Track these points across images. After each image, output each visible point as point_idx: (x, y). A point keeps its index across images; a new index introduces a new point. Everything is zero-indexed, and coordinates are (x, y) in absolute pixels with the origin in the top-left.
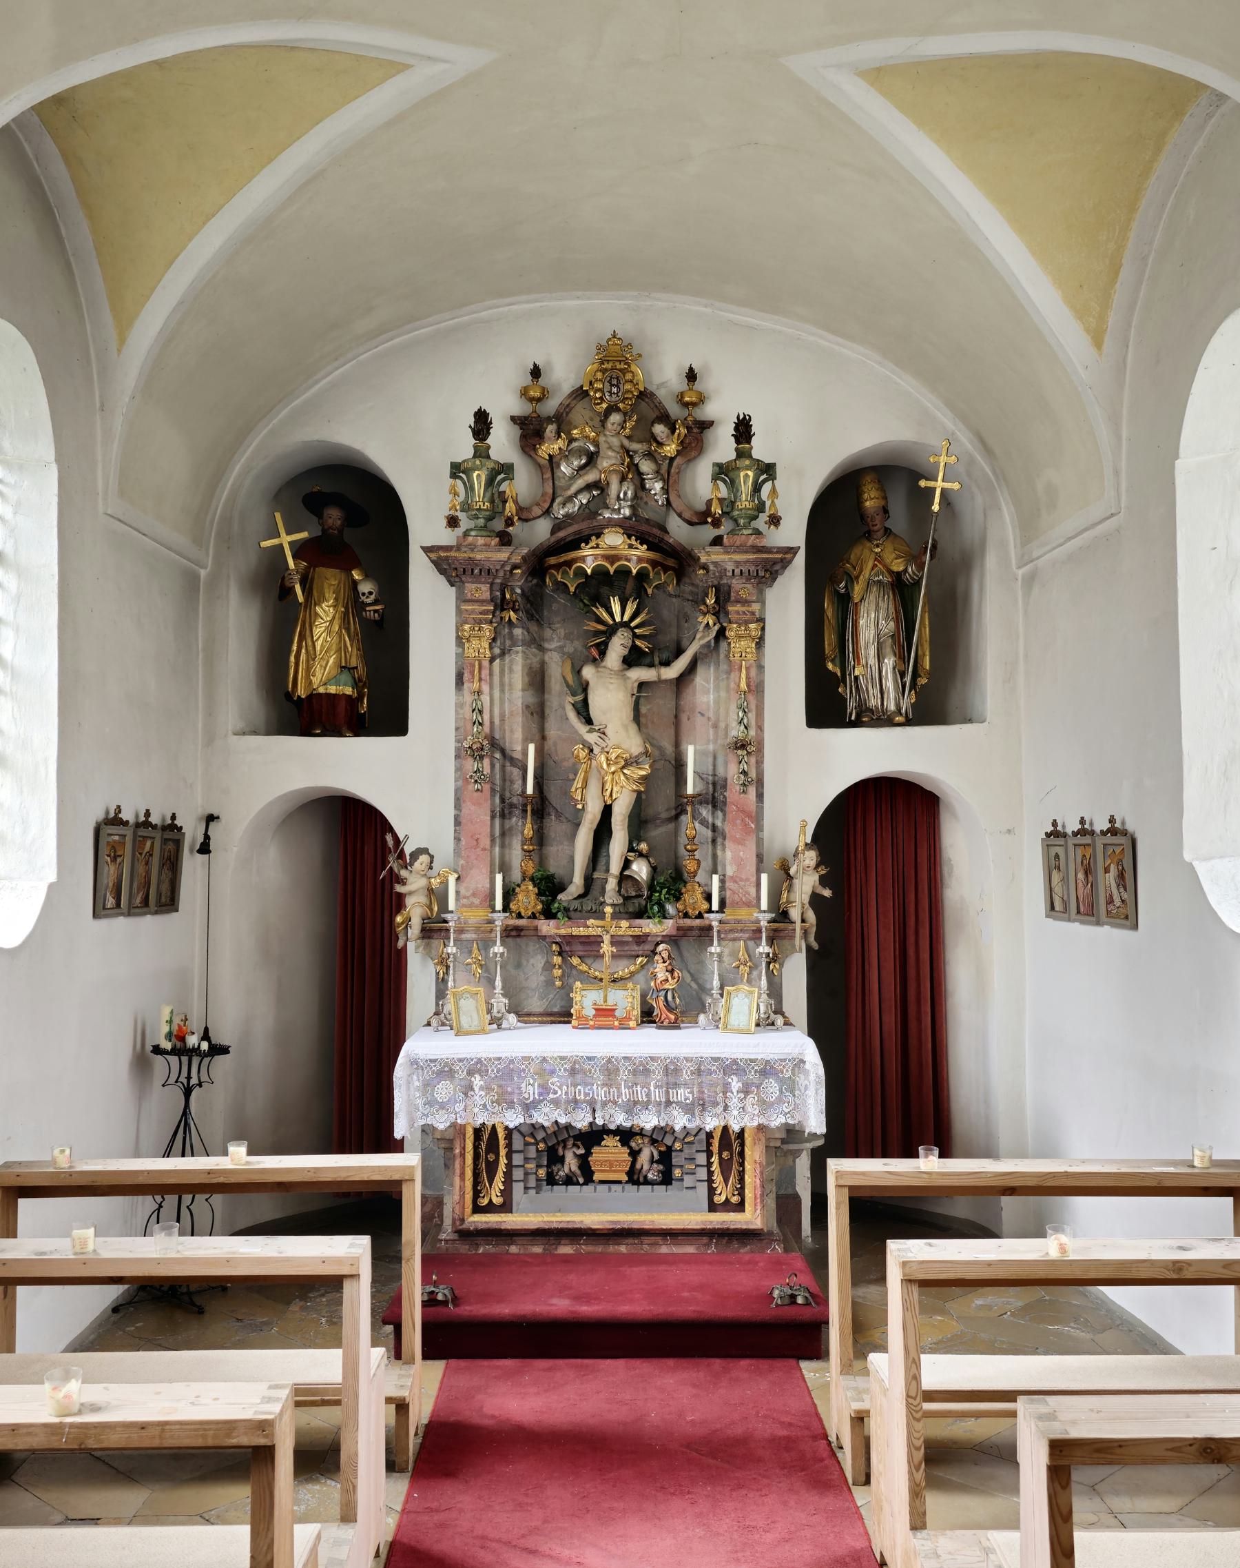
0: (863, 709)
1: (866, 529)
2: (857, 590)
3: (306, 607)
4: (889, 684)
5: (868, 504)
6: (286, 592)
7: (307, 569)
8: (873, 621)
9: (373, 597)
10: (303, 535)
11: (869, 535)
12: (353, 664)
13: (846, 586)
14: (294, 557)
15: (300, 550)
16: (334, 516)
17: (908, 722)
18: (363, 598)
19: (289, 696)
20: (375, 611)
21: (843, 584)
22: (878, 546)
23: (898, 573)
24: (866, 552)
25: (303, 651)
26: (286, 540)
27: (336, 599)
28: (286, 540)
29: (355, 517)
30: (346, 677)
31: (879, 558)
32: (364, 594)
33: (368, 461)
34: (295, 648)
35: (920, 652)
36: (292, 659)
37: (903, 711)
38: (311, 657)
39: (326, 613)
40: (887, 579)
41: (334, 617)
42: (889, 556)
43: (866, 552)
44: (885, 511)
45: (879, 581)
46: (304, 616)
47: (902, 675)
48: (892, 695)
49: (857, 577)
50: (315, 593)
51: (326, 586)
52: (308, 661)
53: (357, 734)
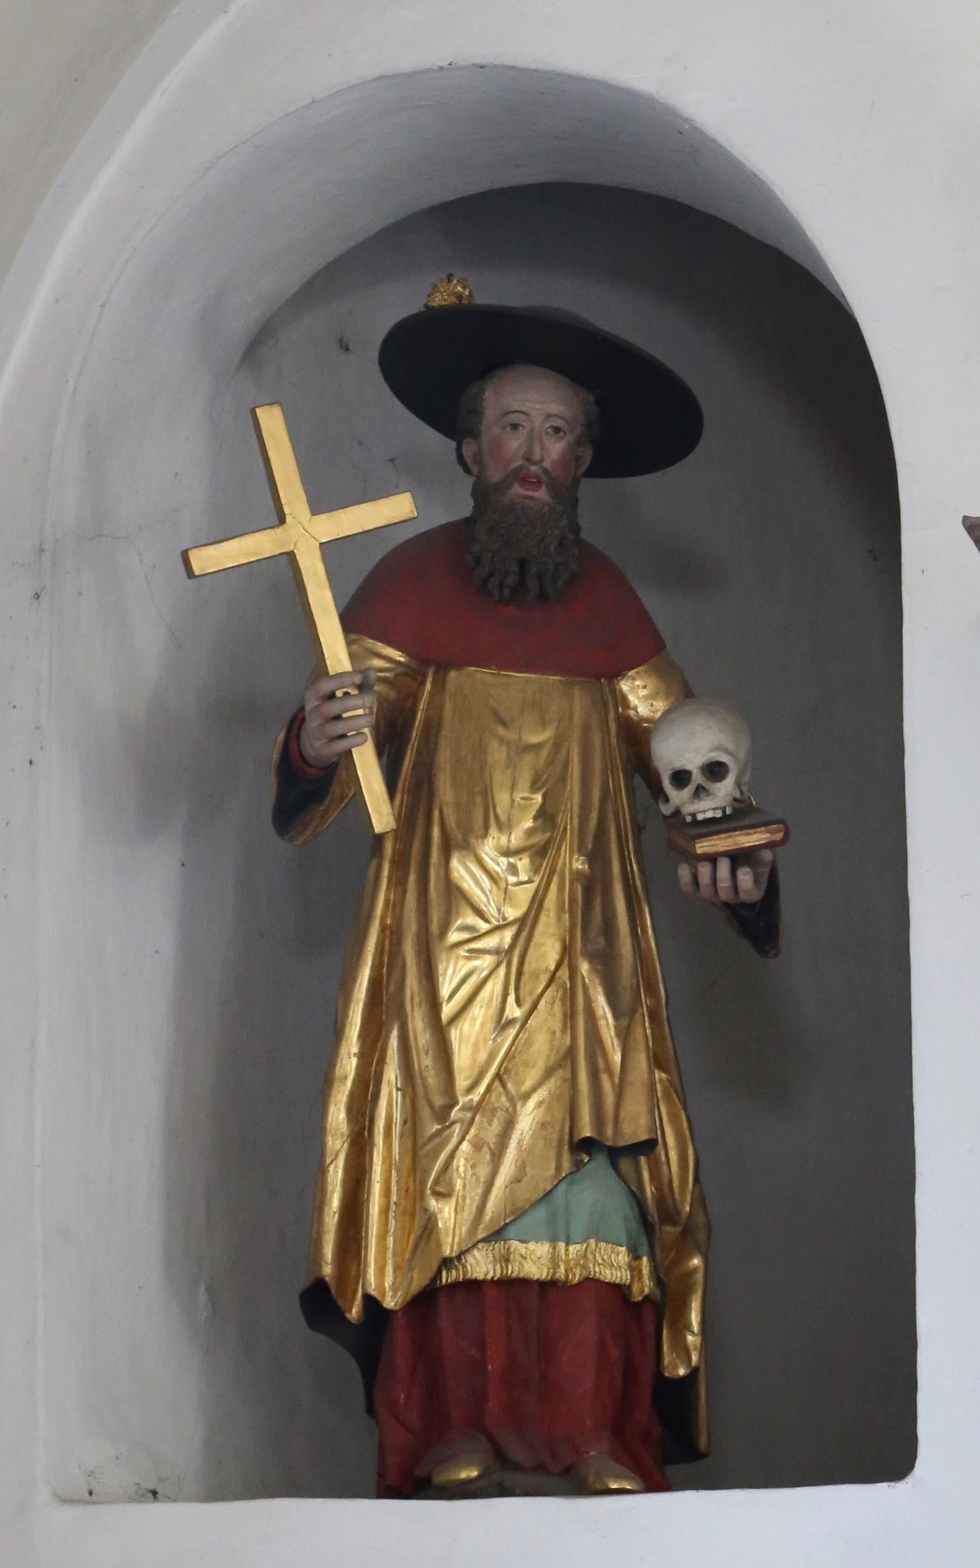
3: (400, 864)
6: (306, 788)
7: (407, 680)
9: (725, 790)
10: (394, 510)
12: (635, 1127)
14: (353, 621)
15: (382, 591)
16: (533, 413)
18: (678, 797)
19: (319, 1302)
20: (738, 858)
25: (392, 1074)
26: (308, 534)
27: (546, 816)
28: (308, 534)
29: (638, 418)
30: (598, 1191)
32: (681, 778)
33: (810, 250)
34: (348, 1063)
36: (338, 1115)
38: (432, 1105)
39: (494, 876)
41: (537, 903)
46: (396, 907)
50: (446, 791)
51: (497, 754)
52: (412, 1122)
53: (655, 1482)
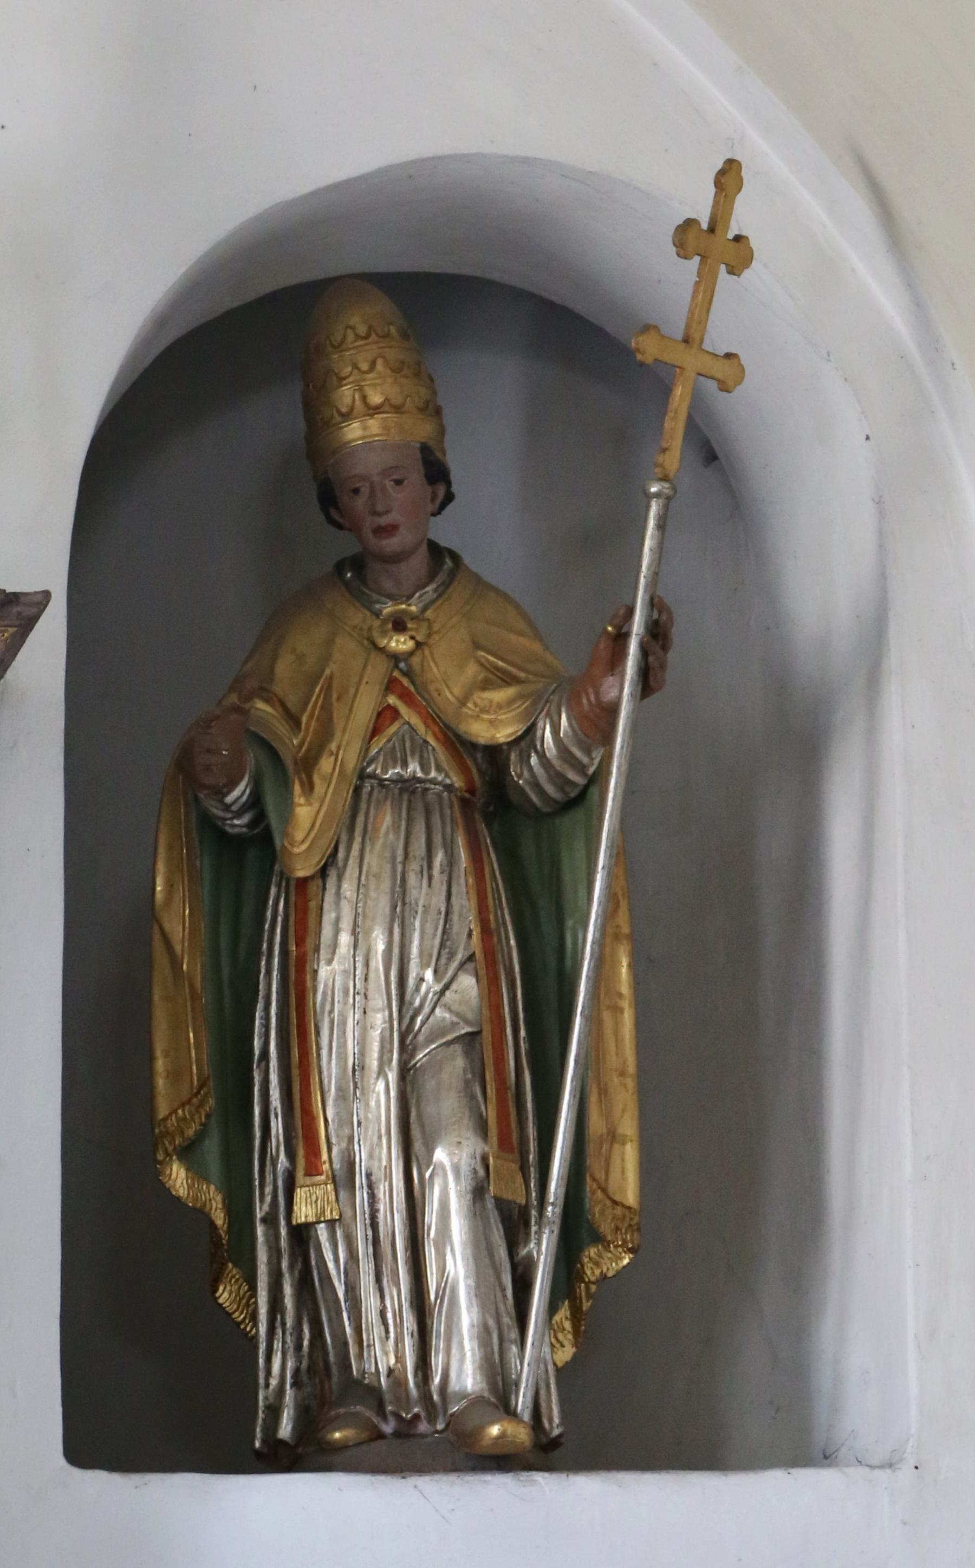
0: (330, 1382)
1: (346, 545)
2: (306, 820)
4: (455, 1264)
5: (354, 432)
8: (378, 969)
11: (357, 573)
13: (255, 802)
17: (544, 1453)
21: (239, 792)
22: (399, 625)
23: (494, 755)
24: (347, 649)
31: (403, 679)
35: (595, 1124)
37: (522, 1401)
40: (441, 773)
42: (450, 674)
43: (347, 649)
44: (436, 472)
45: (407, 786)
47: (516, 1223)
48: (467, 1317)
49: (308, 765)
